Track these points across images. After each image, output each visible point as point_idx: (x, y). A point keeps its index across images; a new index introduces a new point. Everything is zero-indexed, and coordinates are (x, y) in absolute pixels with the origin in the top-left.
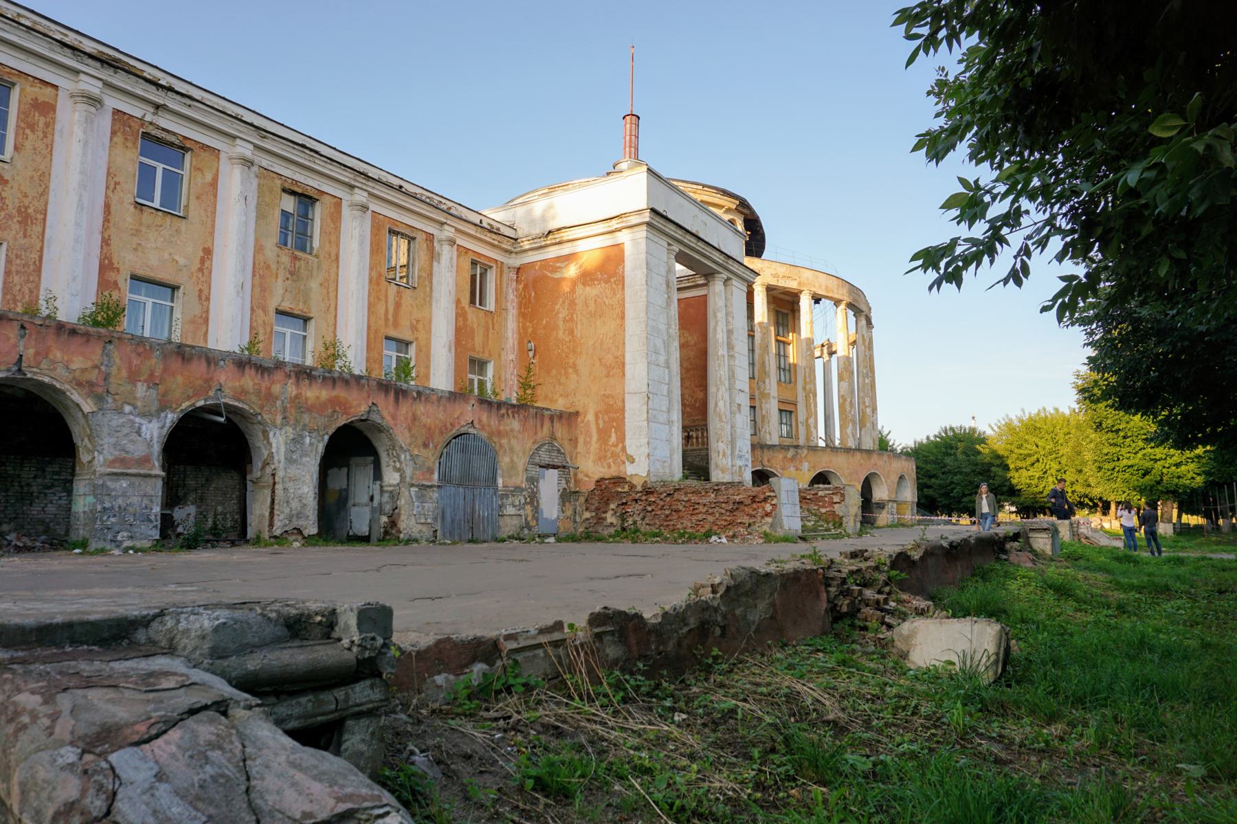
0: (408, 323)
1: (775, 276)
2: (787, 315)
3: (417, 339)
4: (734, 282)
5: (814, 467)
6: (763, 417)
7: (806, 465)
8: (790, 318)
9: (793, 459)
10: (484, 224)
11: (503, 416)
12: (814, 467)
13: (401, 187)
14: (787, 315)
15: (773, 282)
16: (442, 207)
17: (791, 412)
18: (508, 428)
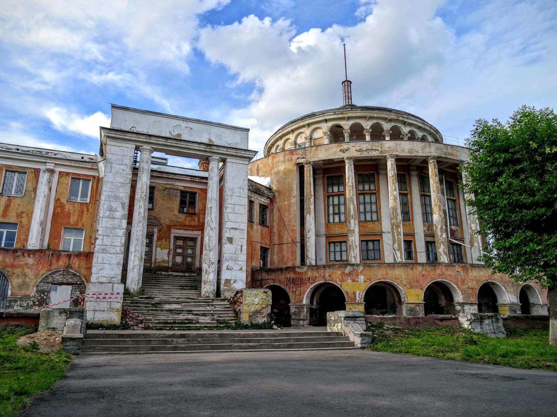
0: (15, 214)
1: (360, 150)
2: (373, 174)
3: (21, 222)
4: (228, 160)
5: (369, 279)
6: (350, 246)
7: (362, 278)
8: (407, 177)
9: (349, 274)
10: (86, 159)
11: (19, 256)
12: (369, 279)
13: (18, 150)
14: (373, 174)
15: (358, 155)
16: (49, 155)
17: (379, 240)
18: (22, 263)
